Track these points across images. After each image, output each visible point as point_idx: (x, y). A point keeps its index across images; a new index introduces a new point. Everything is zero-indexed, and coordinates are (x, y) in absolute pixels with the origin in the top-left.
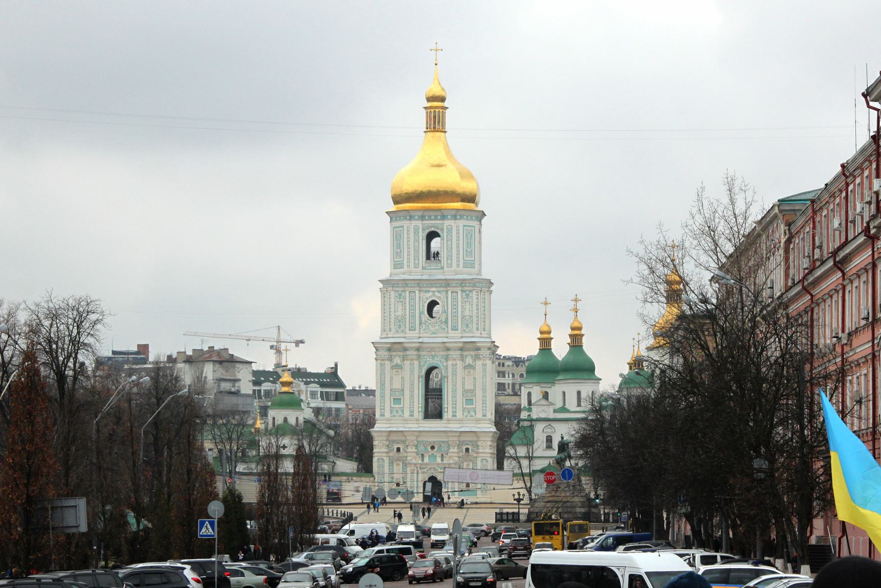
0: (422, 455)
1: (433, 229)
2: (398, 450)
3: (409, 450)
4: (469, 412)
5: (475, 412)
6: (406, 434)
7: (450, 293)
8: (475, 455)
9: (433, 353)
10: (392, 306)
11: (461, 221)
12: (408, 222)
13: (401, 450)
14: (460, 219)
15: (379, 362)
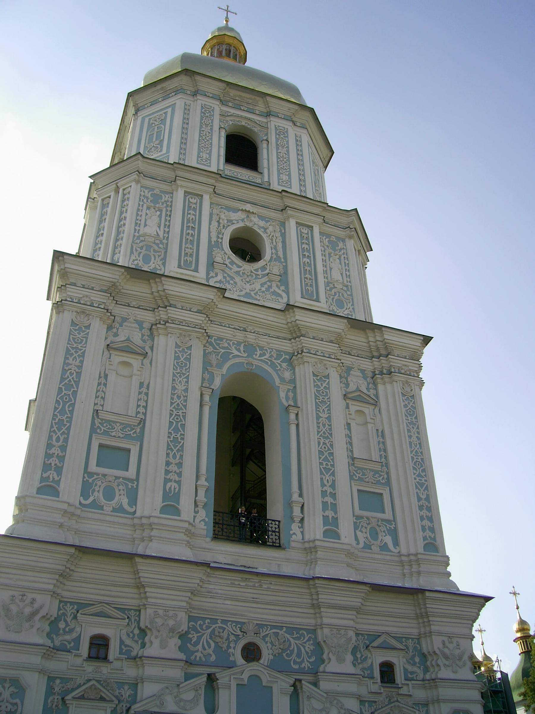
0: (211, 678)
1: (243, 124)
2: (99, 647)
3: (153, 649)
4: (374, 534)
5: (394, 534)
6: (148, 571)
7: (292, 224)
8: (420, 694)
9: (251, 338)
10: (130, 215)
11: (305, 131)
12: (191, 98)
13: (113, 652)
14: (303, 127)
15: (68, 316)
